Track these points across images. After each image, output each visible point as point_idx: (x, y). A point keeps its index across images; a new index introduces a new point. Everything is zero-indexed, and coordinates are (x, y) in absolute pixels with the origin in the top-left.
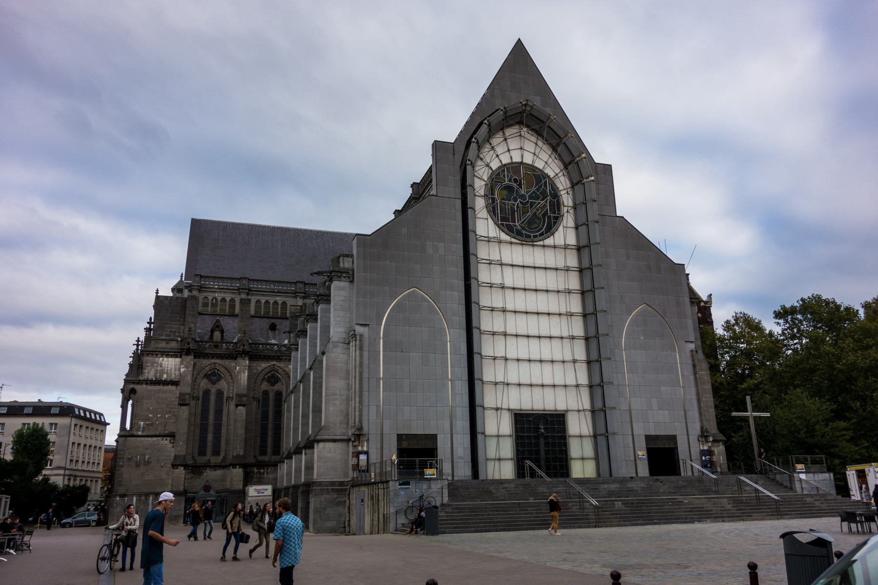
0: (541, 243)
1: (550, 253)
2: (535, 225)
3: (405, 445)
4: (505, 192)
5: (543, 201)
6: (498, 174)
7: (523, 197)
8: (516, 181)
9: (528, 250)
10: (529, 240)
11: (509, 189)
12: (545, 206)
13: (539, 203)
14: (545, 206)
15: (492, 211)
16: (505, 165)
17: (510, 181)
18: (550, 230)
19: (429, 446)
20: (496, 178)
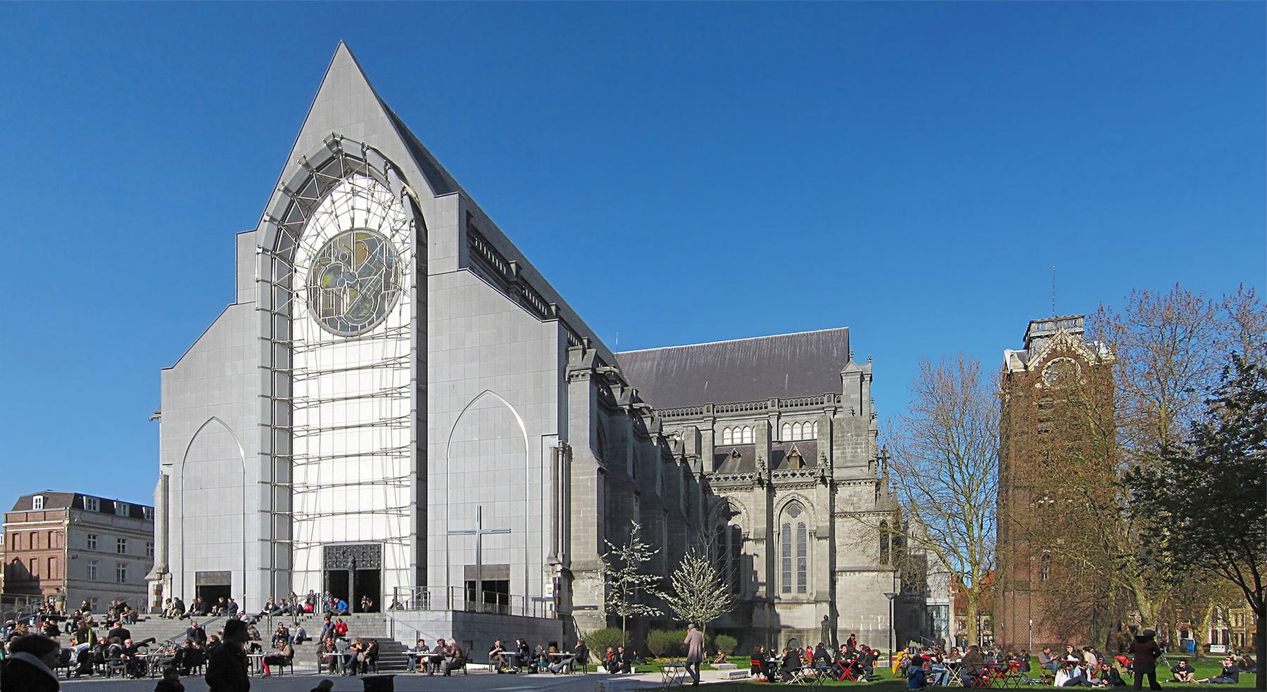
0: (370, 333)
1: (379, 344)
2: (365, 311)
3: (203, 583)
4: (330, 277)
5: (375, 275)
6: (323, 255)
7: (353, 276)
8: (344, 256)
9: (354, 346)
10: (355, 333)
11: (336, 270)
12: (379, 281)
13: (371, 279)
14: (379, 281)
15: (313, 303)
16: (331, 240)
17: (337, 258)
18: (381, 314)
19: (225, 583)
20: (321, 260)
